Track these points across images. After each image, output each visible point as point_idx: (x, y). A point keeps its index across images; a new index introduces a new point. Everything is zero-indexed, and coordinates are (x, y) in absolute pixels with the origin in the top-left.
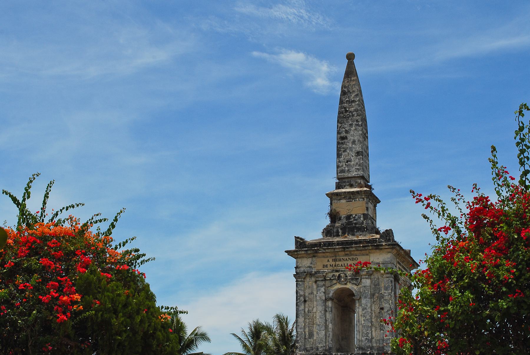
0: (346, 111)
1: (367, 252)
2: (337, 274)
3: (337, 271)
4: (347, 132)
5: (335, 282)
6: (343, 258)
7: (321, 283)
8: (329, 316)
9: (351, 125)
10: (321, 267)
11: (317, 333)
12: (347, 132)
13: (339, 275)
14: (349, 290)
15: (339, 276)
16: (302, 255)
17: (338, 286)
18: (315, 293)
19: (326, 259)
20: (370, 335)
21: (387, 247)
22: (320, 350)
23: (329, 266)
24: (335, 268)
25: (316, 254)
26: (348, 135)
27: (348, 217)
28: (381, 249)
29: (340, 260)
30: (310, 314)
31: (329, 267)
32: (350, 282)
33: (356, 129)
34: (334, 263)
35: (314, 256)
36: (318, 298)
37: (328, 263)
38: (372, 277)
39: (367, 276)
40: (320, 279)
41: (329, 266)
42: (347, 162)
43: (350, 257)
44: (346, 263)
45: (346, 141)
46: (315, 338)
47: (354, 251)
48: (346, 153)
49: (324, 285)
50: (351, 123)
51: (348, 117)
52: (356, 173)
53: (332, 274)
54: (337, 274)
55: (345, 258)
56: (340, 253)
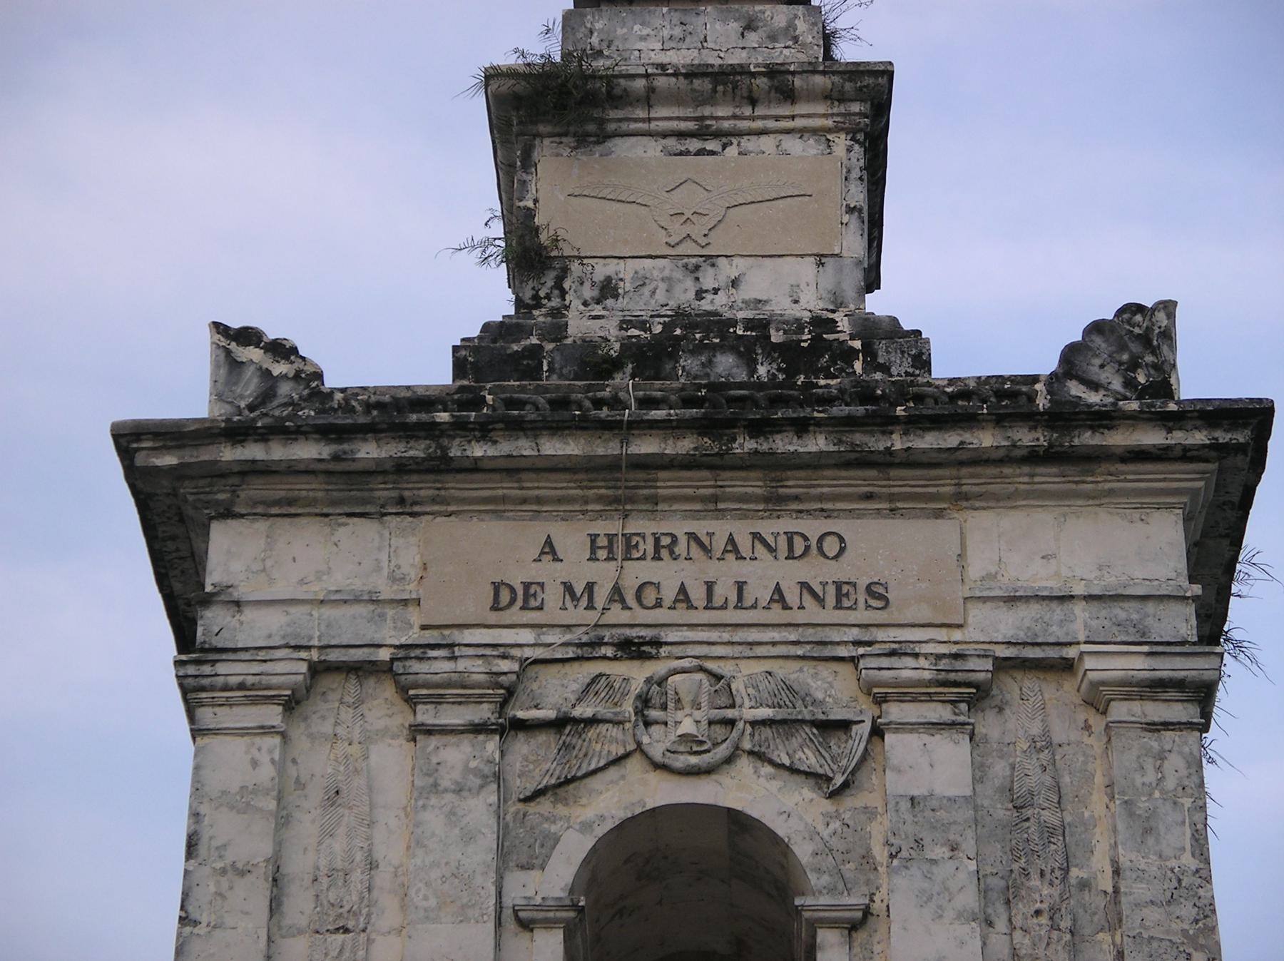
3: (633, 649)
6: (701, 527)
7: (457, 756)
10: (475, 604)
14: (737, 821)
23: (552, 596)
24: (617, 615)
29: (663, 548)
32: (759, 756)
34: (604, 574)
37: (547, 572)
38: (988, 724)
41: (552, 596)
43: (768, 528)
44: (726, 573)
47: (814, 463)
54: (637, 674)
55: (719, 529)
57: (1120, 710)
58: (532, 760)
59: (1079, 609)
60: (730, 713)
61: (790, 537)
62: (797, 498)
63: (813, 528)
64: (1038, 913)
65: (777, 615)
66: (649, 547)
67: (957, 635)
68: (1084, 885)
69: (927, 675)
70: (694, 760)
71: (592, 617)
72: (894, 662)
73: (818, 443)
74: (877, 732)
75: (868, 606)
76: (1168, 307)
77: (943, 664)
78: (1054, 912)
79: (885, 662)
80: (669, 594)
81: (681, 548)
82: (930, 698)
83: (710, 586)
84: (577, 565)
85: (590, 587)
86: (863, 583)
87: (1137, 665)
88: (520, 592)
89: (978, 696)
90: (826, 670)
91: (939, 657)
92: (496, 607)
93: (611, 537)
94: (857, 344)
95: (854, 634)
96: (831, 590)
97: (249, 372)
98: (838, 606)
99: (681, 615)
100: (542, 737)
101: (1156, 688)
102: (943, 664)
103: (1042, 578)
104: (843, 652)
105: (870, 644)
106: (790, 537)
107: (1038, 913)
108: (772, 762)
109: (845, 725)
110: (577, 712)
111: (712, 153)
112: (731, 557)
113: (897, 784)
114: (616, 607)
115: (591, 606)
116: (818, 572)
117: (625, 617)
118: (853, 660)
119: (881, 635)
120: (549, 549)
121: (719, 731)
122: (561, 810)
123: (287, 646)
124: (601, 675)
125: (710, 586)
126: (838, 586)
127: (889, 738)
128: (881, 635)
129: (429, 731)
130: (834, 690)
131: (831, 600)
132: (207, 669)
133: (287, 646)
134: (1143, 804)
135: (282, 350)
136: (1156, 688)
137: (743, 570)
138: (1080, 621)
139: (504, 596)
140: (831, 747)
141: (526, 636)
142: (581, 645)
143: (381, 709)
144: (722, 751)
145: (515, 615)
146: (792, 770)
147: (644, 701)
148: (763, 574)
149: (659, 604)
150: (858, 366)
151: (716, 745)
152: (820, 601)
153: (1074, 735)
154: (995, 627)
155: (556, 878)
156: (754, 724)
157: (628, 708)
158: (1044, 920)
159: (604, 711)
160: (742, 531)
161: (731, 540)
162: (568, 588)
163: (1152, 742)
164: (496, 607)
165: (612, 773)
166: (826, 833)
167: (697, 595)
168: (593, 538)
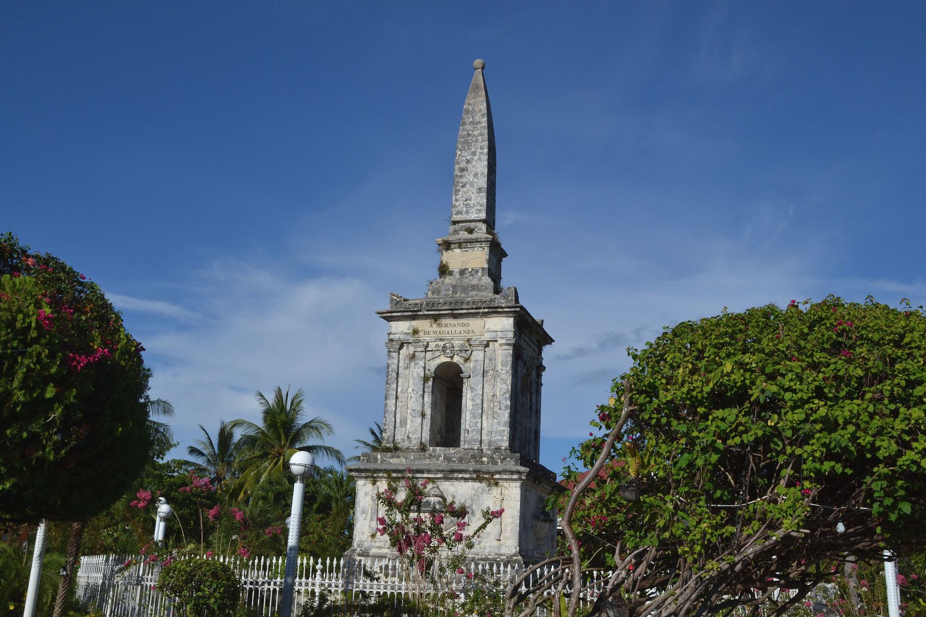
2: (442, 343)
3: (441, 340)
4: (468, 161)
5: (438, 353)
8: (428, 399)
9: (474, 153)
11: (412, 421)
20: (479, 425)
26: (469, 166)
29: (446, 326)
31: (432, 334)
33: (480, 159)
36: (415, 375)
40: (419, 350)
44: (454, 329)
46: (408, 427)
48: (465, 189)
54: (442, 343)
116: (465, 328)
148: (458, 329)
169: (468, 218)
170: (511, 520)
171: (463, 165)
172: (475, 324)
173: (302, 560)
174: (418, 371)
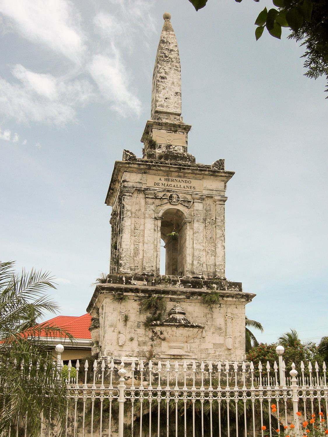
0: (166, 57)
1: (202, 176)
3: (168, 191)
5: (166, 201)
12: (166, 73)
13: (171, 195)
14: (178, 210)
15: (171, 197)
16: (132, 169)
17: (168, 206)
18: (143, 210)
19: (159, 177)
21: (223, 175)
22: (147, 269)
23: (161, 184)
24: (167, 187)
25: (148, 171)
27: (168, 146)
28: (217, 176)
29: (172, 181)
30: (136, 231)
31: (161, 186)
34: (166, 183)
35: (145, 173)
37: (160, 182)
38: (204, 202)
39: (199, 201)
41: (161, 184)
42: (166, 99)
43: (183, 179)
44: (179, 184)
45: (165, 80)
47: (189, 173)
48: (165, 91)
49: (153, 203)
50: (170, 67)
51: (168, 62)
52: (175, 110)
53: (163, 193)
55: (178, 179)
56: (173, 174)
57: (217, 202)
58: (157, 202)
59: (214, 191)
60: (179, 199)
61: (185, 181)
62: (186, 176)
63: (188, 180)
64: (208, 222)
65: (184, 189)
66: (171, 180)
67: (202, 193)
68: (212, 220)
69: (199, 197)
70: (175, 204)
71: (165, 187)
72: (196, 195)
73: (190, 171)
74: (193, 203)
75: (193, 189)
76: (224, 160)
77: (201, 196)
78: (210, 222)
79: (195, 195)
80: (173, 186)
81: (174, 181)
82: (199, 199)
83: (177, 185)
84: (163, 181)
85: (165, 184)
86: (193, 187)
87: (220, 198)
88: (157, 183)
89: (203, 199)
90: (188, 195)
91: (200, 195)
92: (155, 185)
93: (167, 179)
94: (188, 157)
95: (192, 192)
96: (190, 187)
97: (128, 156)
98: (190, 189)
99: (174, 188)
100: (159, 200)
101: (221, 200)
102: (201, 196)
103: (211, 188)
104: (190, 194)
105: (193, 193)
106: (185, 181)
107: (208, 222)
108: (182, 205)
109: (190, 202)
110: (163, 197)
111: (171, 133)
112: (179, 182)
113: (195, 208)
114: (167, 186)
115: (165, 186)
117: (168, 188)
118: (191, 195)
119: (194, 192)
120: (160, 179)
121: (178, 201)
122: (161, 208)
123: (132, 187)
124: (165, 194)
125: (177, 185)
126: (190, 186)
127: (195, 203)
128: (194, 192)
129: (147, 198)
130: (189, 198)
131: (189, 188)
132: (125, 189)
133: (132, 187)
134: (219, 212)
135: (131, 153)
136: (221, 200)
137: (181, 184)
138: (214, 193)
139: (155, 184)
140: (186, 203)
141: (158, 189)
142: (164, 190)
143: (142, 196)
144: (178, 203)
145: (156, 186)
146: (185, 206)
147: (170, 197)
148: (183, 184)
149: (172, 187)
150: (188, 160)
151: (177, 202)
152: (188, 188)
153: (213, 204)
154: (205, 192)
155: (160, 214)
156: (181, 200)
157: (168, 197)
158: (209, 223)
159: (166, 198)
160: (181, 179)
161: (179, 180)
162: (162, 184)
163: (220, 206)
164: (155, 185)
165: (166, 204)
166: (188, 212)
167: (176, 186)
168: (165, 178)
169: (168, 111)
170: (239, 334)
171: (163, 75)
172: (195, 183)
173: (313, 366)
174: (150, 212)
